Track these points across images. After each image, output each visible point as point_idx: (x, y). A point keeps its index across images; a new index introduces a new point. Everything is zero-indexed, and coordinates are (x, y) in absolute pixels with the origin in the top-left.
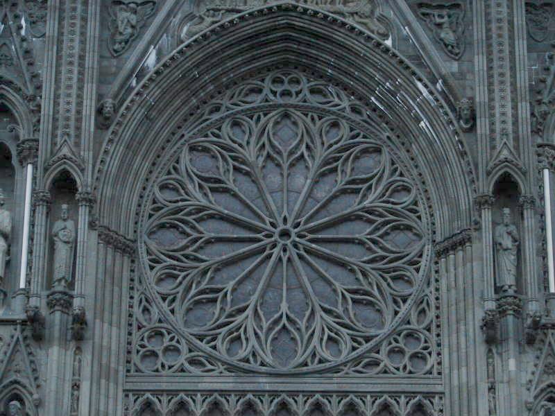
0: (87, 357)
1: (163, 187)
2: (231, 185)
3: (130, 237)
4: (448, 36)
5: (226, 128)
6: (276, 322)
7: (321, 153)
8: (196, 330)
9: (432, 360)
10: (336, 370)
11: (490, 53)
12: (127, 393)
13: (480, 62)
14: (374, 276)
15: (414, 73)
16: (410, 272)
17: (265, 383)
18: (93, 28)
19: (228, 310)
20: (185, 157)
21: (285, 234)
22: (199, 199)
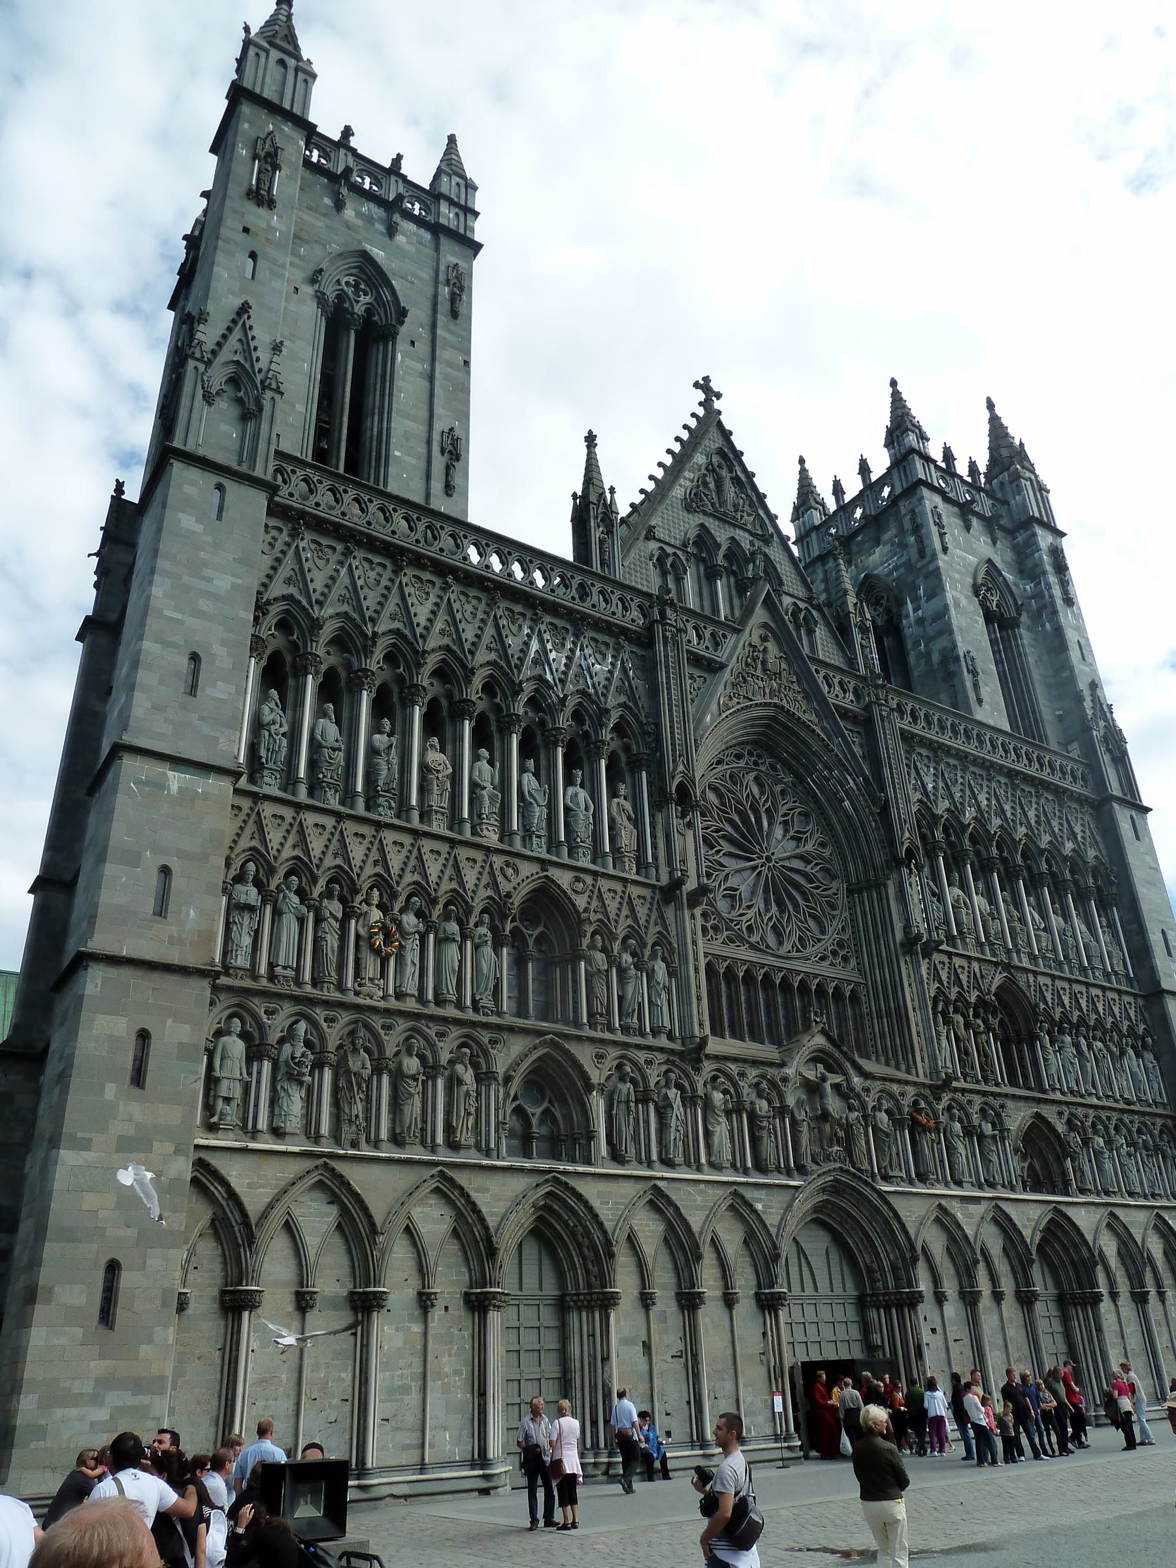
6: (770, 919)
9: (853, 962)
11: (891, 768)
15: (847, 770)
19: (744, 905)
21: (768, 859)
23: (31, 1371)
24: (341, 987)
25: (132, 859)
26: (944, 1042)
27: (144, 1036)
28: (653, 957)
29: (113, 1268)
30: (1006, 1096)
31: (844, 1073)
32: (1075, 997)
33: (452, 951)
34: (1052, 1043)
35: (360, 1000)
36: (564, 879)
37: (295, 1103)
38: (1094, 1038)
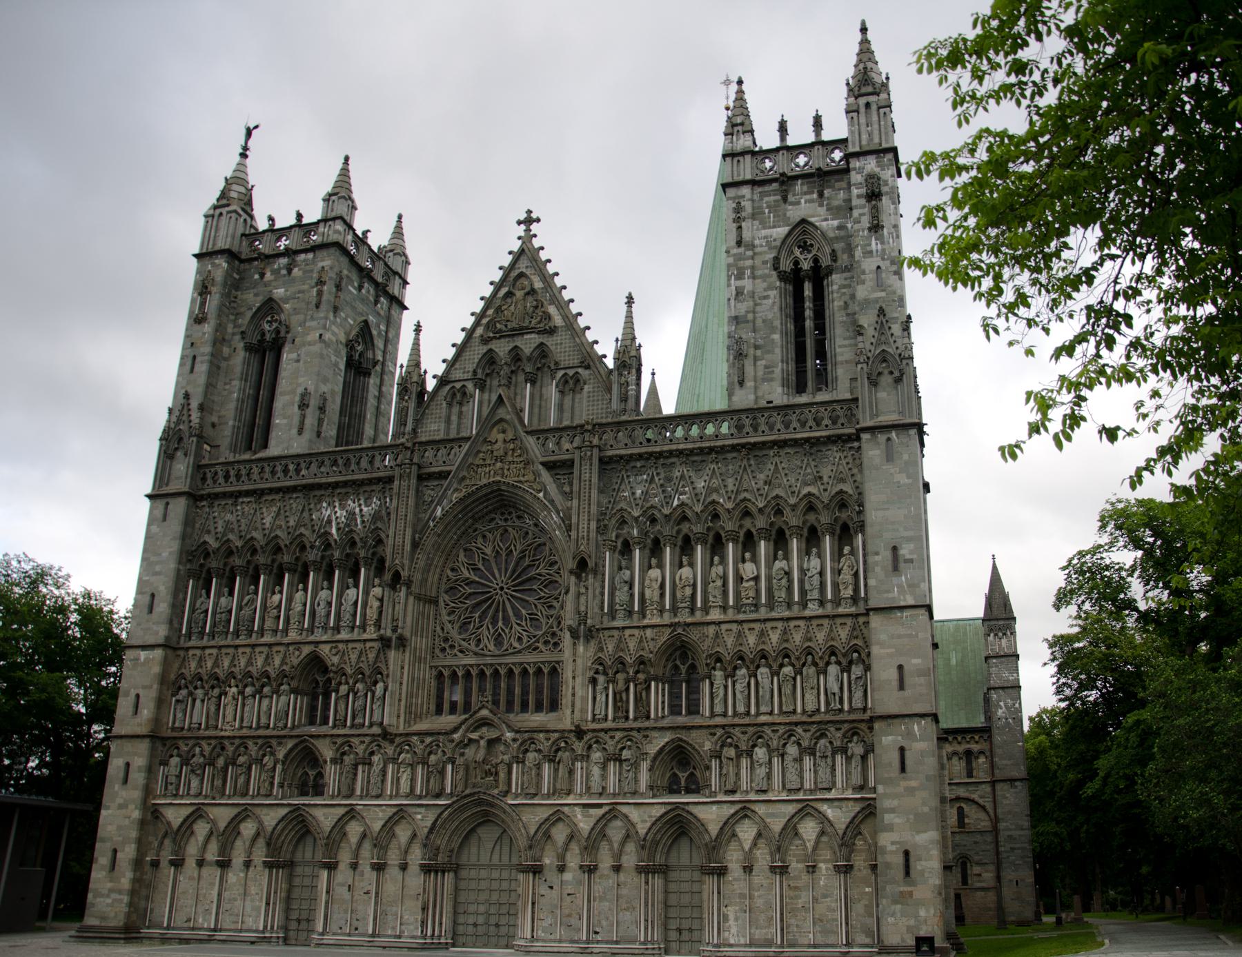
0: (407, 654)
1: (453, 570)
2: (480, 566)
3: (434, 595)
4: (567, 489)
5: (480, 540)
7: (519, 548)
8: (463, 636)
10: (519, 652)
12: (431, 667)
13: (575, 502)
14: (539, 606)
16: (555, 603)
17: (489, 660)
18: (412, 502)
20: (462, 554)
21: (502, 589)
22: (466, 574)
23: (91, 886)
24: (216, 727)
25: (127, 694)
26: (601, 698)
27: (128, 765)
28: (375, 683)
29: (115, 851)
30: (647, 728)
31: (500, 730)
32: (762, 634)
33: (265, 702)
34: (726, 678)
35: (223, 733)
36: (325, 650)
37: (195, 783)
38: (782, 666)
